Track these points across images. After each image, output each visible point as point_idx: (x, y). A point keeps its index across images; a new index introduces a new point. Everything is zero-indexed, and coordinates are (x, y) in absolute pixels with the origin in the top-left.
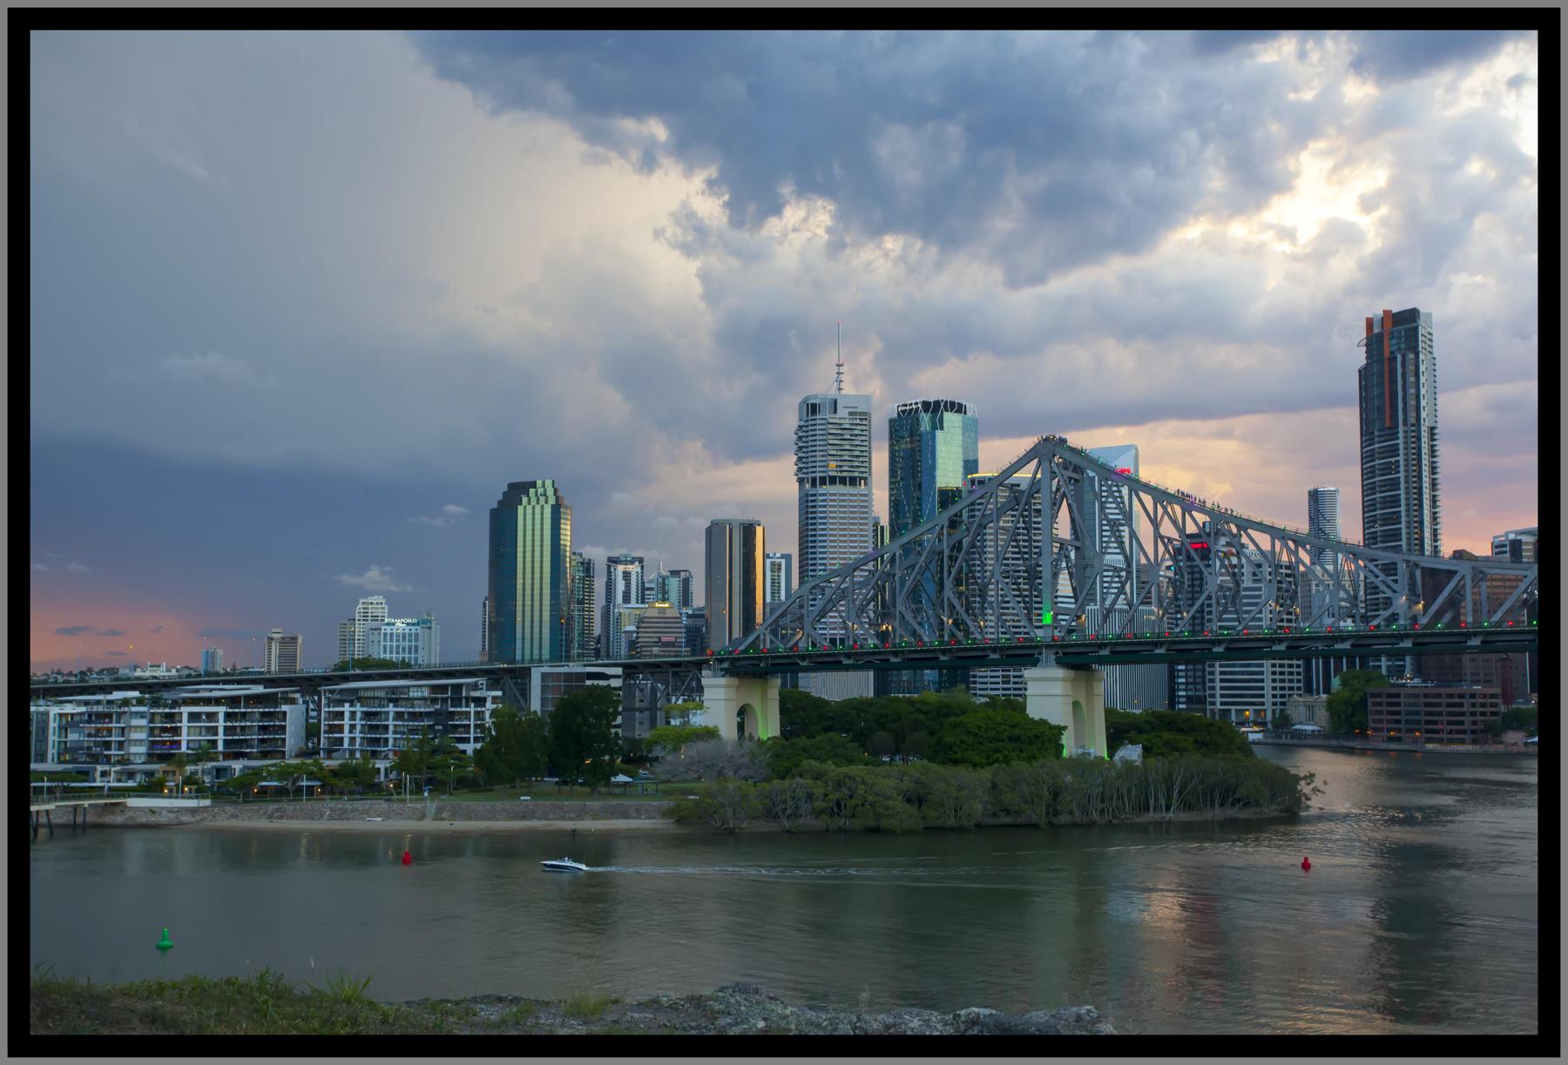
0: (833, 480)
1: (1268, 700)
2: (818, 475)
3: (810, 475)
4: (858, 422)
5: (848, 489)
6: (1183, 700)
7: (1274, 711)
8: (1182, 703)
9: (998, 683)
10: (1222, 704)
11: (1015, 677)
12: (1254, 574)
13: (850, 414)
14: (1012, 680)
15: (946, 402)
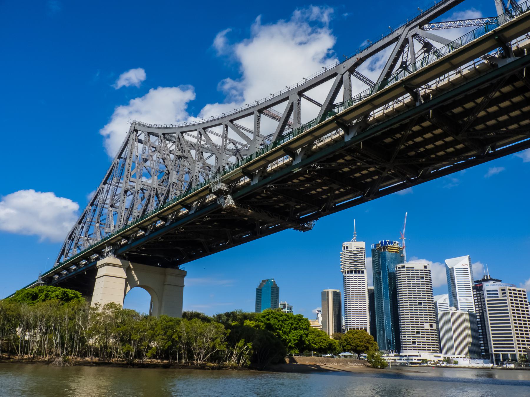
0: (352, 272)
1: (516, 350)
2: (347, 270)
3: (344, 270)
4: (360, 251)
5: (357, 275)
6: (483, 351)
7: (520, 355)
8: (483, 352)
9: (411, 345)
10: (495, 351)
11: (418, 342)
12: (503, 293)
13: (357, 248)
14: (417, 343)
15: (389, 242)
